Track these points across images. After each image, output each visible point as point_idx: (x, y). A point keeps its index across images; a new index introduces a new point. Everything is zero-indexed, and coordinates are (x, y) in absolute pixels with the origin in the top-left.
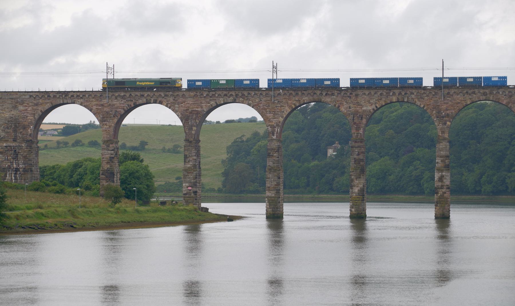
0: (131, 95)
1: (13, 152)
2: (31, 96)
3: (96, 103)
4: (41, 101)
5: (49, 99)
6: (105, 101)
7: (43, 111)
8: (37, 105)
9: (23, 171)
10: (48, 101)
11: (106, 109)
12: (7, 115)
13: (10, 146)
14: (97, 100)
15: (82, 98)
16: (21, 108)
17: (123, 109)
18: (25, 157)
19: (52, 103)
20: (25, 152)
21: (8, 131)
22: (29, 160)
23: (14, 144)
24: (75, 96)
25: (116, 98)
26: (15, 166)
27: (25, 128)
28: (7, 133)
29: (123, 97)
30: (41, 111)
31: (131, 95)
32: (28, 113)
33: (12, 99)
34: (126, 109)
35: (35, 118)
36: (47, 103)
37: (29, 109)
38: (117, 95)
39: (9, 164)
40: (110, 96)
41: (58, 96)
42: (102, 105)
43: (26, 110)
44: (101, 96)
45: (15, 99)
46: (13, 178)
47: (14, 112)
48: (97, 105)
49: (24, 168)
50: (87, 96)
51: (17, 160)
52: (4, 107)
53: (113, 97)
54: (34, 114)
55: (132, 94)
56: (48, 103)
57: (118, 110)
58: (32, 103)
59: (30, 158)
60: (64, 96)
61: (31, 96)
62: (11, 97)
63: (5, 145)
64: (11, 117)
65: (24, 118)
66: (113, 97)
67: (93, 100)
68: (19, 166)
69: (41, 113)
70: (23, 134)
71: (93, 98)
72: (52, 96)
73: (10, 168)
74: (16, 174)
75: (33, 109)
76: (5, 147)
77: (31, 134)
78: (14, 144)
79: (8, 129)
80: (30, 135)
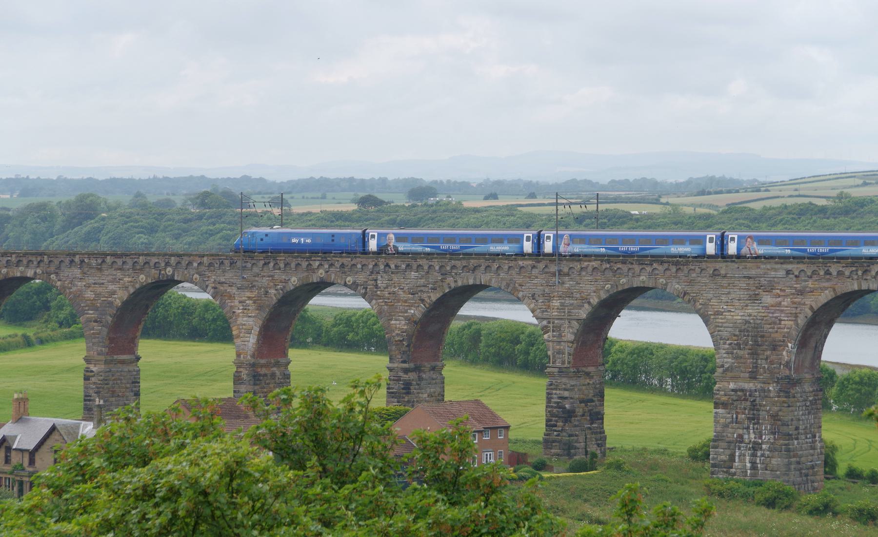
1: (748, 403)
2: (788, 272)
4: (810, 284)
5: (828, 280)
7: (816, 308)
8: (801, 292)
9: (770, 450)
10: (826, 284)
12: (738, 316)
13: (742, 390)
16: (768, 299)
18: (775, 417)
19: (834, 290)
20: (774, 404)
21: (740, 353)
22: (783, 425)
23: (751, 385)
26: (752, 436)
28: (737, 357)
30: (811, 308)
32: (782, 311)
33: (749, 278)
35: (797, 325)
36: (823, 289)
37: (785, 303)
39: (741, 431)
41: (847, 273)
45: (754, 278)
46: (748, 465)
49: (772, 444)
51: (758, 423)
56: (826, 288)
59: (786, 419)
60: (860, 273)
61: (788, 272)
62: (746, 273)
63: (732, 386)
64: (747, 322)
65: (775, 323)
68: (761, 438)
69: (810, 314)
70: (772, 363)
72: (835, 273)
73: (742, 442)
74: (754, 455)
76: (733, 390)
77: (788, 363)
78: (749, 386)
79: (740, 349)
80: (787, 365)
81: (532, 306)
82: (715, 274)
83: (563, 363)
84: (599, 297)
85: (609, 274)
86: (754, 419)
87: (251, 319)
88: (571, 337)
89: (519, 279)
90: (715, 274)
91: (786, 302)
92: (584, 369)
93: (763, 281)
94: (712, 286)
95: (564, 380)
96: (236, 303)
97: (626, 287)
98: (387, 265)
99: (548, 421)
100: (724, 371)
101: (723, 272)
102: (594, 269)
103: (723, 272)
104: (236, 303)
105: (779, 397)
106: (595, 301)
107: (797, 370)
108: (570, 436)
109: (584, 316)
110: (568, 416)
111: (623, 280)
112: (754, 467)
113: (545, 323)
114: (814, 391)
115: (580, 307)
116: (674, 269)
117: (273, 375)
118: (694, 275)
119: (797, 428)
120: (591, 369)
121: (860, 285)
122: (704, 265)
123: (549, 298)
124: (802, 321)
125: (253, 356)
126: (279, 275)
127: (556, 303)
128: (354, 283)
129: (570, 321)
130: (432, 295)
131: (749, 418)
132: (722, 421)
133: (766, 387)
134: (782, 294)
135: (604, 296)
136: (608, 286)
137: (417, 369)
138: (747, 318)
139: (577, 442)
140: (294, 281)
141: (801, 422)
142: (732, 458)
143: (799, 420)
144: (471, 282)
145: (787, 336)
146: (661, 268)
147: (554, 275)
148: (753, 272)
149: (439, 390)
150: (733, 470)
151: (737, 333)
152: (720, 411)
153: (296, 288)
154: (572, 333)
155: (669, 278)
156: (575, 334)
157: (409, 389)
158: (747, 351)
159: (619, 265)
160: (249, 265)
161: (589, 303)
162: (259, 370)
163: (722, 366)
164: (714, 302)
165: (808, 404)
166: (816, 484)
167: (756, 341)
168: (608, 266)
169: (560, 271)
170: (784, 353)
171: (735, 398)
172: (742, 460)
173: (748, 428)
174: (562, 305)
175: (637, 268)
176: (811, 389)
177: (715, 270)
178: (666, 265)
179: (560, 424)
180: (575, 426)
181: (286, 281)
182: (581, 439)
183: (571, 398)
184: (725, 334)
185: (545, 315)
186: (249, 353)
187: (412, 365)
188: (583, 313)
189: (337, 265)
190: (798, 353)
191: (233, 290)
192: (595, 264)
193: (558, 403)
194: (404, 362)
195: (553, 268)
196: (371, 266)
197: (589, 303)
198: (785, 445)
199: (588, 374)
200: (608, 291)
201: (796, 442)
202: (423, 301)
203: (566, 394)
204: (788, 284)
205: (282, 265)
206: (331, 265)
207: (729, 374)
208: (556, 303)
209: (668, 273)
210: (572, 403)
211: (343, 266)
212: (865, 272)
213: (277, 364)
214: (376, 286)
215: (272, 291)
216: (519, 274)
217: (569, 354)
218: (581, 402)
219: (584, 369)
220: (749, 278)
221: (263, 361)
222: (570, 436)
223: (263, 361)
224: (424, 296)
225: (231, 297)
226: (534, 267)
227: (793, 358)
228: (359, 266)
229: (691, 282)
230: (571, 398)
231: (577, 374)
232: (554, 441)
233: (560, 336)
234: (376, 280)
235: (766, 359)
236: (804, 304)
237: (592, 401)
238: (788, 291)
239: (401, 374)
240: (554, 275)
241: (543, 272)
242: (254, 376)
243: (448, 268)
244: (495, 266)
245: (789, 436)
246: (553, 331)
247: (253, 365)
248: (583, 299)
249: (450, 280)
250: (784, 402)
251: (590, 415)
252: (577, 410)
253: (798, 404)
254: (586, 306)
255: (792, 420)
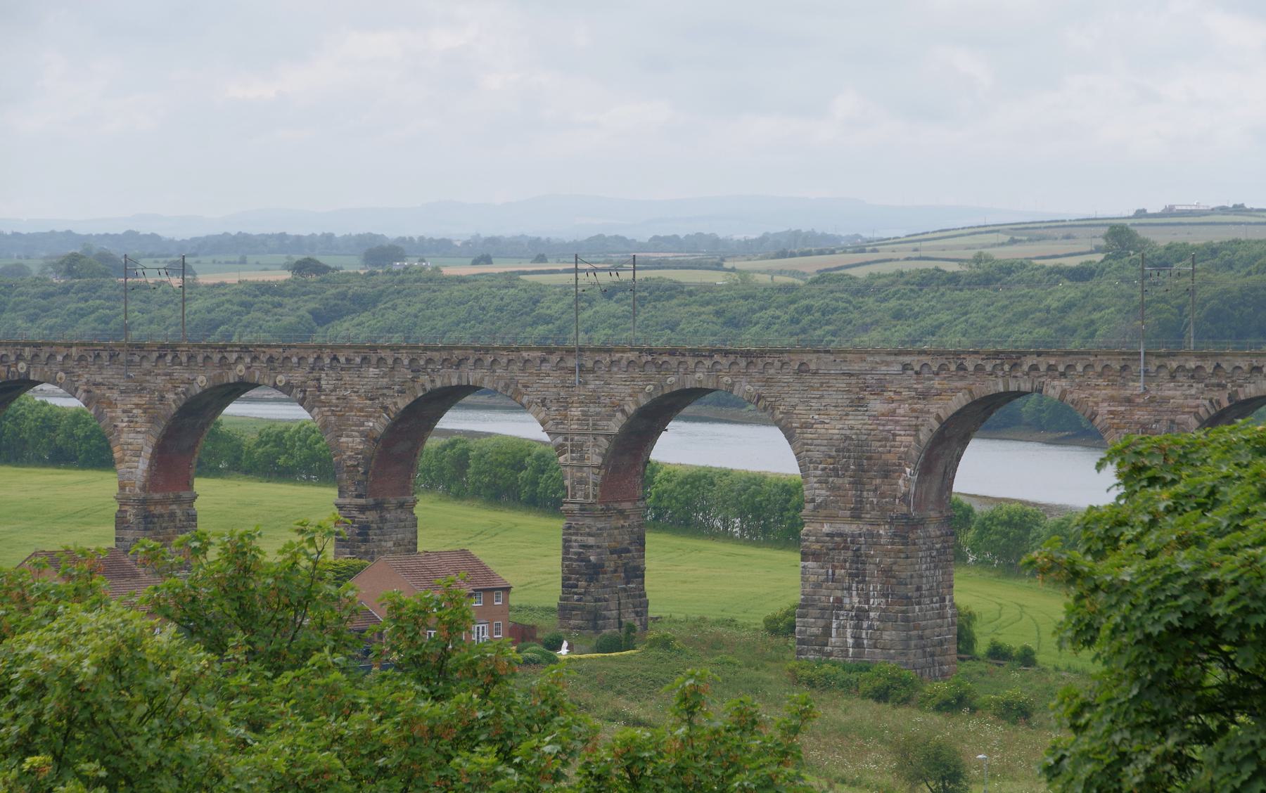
0: (1218, 366)
1: (850, 553)
2: (905, 367)
3: (1109, 392)
4: (936, 383)
5: (963, 378)
6: (1136, 387)
8: (924, 396)
9: (880, 619)
10: (959, 384)
11: (1141, 415)
12: (835, 429)
13: (841, 535)
14: (1113, 384)
15: (1063, 375)
16: (877, 405)
17: (1196, 414)
18: (887, 573)
19: (971, 392)
20: (886, 554)
21: (838, 481)
22: (900, 583)
23: (854, 527)
24: (1043, 368)
25: (1173, 377)
26: (856, 600)
27: (887, 473)
28: (833, 488)
29: (1195, 374)
30: (938, 417)
31: (1218, 366)
32: (897, 422)
33: (851, 375)
34: (1205, 417)
35: (919, 442)
37: (901, 411)
38: (1175, 365)
39: (839, 593)
40: (1152, 368)
41: (989, 368)
42: (1129, 400)
43: (893, 413)
44: (1124, 368)
45: (857, 375)
46: (850, 641)
47: (856, 421)
48: (1112, 399)
49: (884, 610)
50: (1080, 368)
51: (863, 581)
52: (824, 402)
53: (1164, 374)
54: (917, 428)
55: (1224, 365)
56: (959, 390)
57: (1180, 418)
58: (910, 389)
59: (903, 575)
60: (1007, 367)
61: (905, 367)
62: (845, 368)
63: (826, 528)
64: (847, 438)
65: (886, 439)
66: (1164, 374)
67: (1100, 381)
68: (867, 602)
69: (936, 426)
70: (883, 495)
71: (1100, 375)
72: (971, 368)
73: (841, 608)
74: (858, 627)
75: (913, 410)
76: (827, 535)
77: (906, 495)
78: (850, 528)
79: (838, 476)
80: (905, 498)
81: (542, 415)
82: (802, 369)
83: (587, 496)
84: (637, 403)
85: (651, 370)
86: (858, 575)
87: (140, 436)
88: (597, 460)
89: (523, 378)
90: (802, 369)
91: (903, 409)
92: (616, 505)
93: (870, 380)
94: (797, 386)
95: (588, 521)
96: (119, 412)
97: (675, 389)
98: (335, 358)
99: (564, 579)
100: (815, 508)
101: (813, 367)
102: (630, 362)
103: (813, 367)
104: (119, 412)
105: (893, 544)
106: (631, 408)
107: (918, 506)
108: (597, 600)
109: (616, 430)
110: (594, 572)
111: (672, 379)
112: (858, 644)
113: (560, 440)
114: (942, 535)
115: (610, 417)
116: (743, 363)
117: (172, 515)
118: (772, 371)
119: (919, 589)
120: (626, 506)
121: (1006, 384)
122: (786, 357)
123: (565, 404)
124: (924, 436)
125: (143, 488)
126: (180, 373)
127: (576, 412)
128: (288, 383)
129: (595, 437)
130: (398, 400)
131: (850, 575)
132: (813, 578)
133: (875, 529)
134: (897, 397)
135: (644, 401)
136: (650, 388)
137: (379, 506)
138: (848, 432)
139: (607, 609)
140: (201, 381)
141: (924, 580)
142: (827, 631)
143: (921, 577)
144: (454, 382)
145: (905, 457)
146: (725, 362)
147: (573, 371)
148: (856, 367)
149: (409, 536)
150: (828, 649)
151: (834, 453)
152: (810, 564)
153: (205, 391)
154: (599, 454)
155: (736, 375)
156: (604, 456)
157: (367, 535)
158: (847, 480)
159: (665, 358)
160: (137, 359)
161: (623, 411)
162: (152, 508)
163: (813, 501)
164: (801, 409)
165: (934, 553)
166: (946, 667)
167: (860, 465)
168: (650, 358)
169: (581, 366)
170: (901, 482)
171: (830, 545)
172: (841, 634)
173: (849, 589)
174: (585, 414)
175: (691, 362)
176: (938, 533)
177: (802, 364)
178: (732, 357)
179: (582, 583)
180: (604, 587)
181: (191, 382)
182: (613, 605)
183: (598, 547)
184: (816, 455)
185: (561, 428)
186: (139, 484)
187: (371, 501)
188: (615, 426)
189: (264, 358)
190: (919, 482)
191: (115, 395)
192: (631, 356)
193: (580, 554)
194: (359, 496)
195: (571, 362)
196: (311, 360)
197: (623, 411)
198: (902, 612)
199: (621, 513)
200: (650, 394)
201: (917, 608)
202: (385, 409)
203: (591, 541)
204: (905, 383)
205: (184, 359)
206: (255, 358)
207: (822, 512)
208: (576, 412)
209: (735, 368)
210: (600, 554)
211: (271, 360)
212: (1014, 366)
213: (178, 500)
214: (319, 388)
215: (170, 396)
216: (523, 370)
217: (595, 485)
218: (612, 553)
219: (616, 505)
220: (851, 375)
221: (157, 496)
222: (597, 600)
223: (157, 496)
224: (388, 402)
225: (111, 404)
226: (543, 360)
227: (913, 489)
228: (295, 360)
229: (768, 382)
230: (598, 547)
231: (606, 513)
232: (574, 609)
233: (582, 458)
234: (319, 380)
235: (875, 490)
236: (928, 412)
237: (628, 551)
238: (905, 393)
239: (355, 513)
240: (573, 371)
241: (558, 367)
242: (145, 517)
243: (422, 362)
244: (489, 359)
245: (907, 599)
246: (572, 452)
247: (144, 502)
248: (613, 405)
249: (424, 379)
250: (900, 551)
251: (625, 571)
252: (607, 564)
253: (921, 554)
254: (619, 415)
255: (912, 576)
